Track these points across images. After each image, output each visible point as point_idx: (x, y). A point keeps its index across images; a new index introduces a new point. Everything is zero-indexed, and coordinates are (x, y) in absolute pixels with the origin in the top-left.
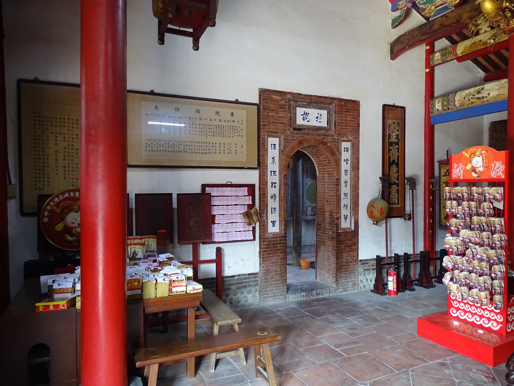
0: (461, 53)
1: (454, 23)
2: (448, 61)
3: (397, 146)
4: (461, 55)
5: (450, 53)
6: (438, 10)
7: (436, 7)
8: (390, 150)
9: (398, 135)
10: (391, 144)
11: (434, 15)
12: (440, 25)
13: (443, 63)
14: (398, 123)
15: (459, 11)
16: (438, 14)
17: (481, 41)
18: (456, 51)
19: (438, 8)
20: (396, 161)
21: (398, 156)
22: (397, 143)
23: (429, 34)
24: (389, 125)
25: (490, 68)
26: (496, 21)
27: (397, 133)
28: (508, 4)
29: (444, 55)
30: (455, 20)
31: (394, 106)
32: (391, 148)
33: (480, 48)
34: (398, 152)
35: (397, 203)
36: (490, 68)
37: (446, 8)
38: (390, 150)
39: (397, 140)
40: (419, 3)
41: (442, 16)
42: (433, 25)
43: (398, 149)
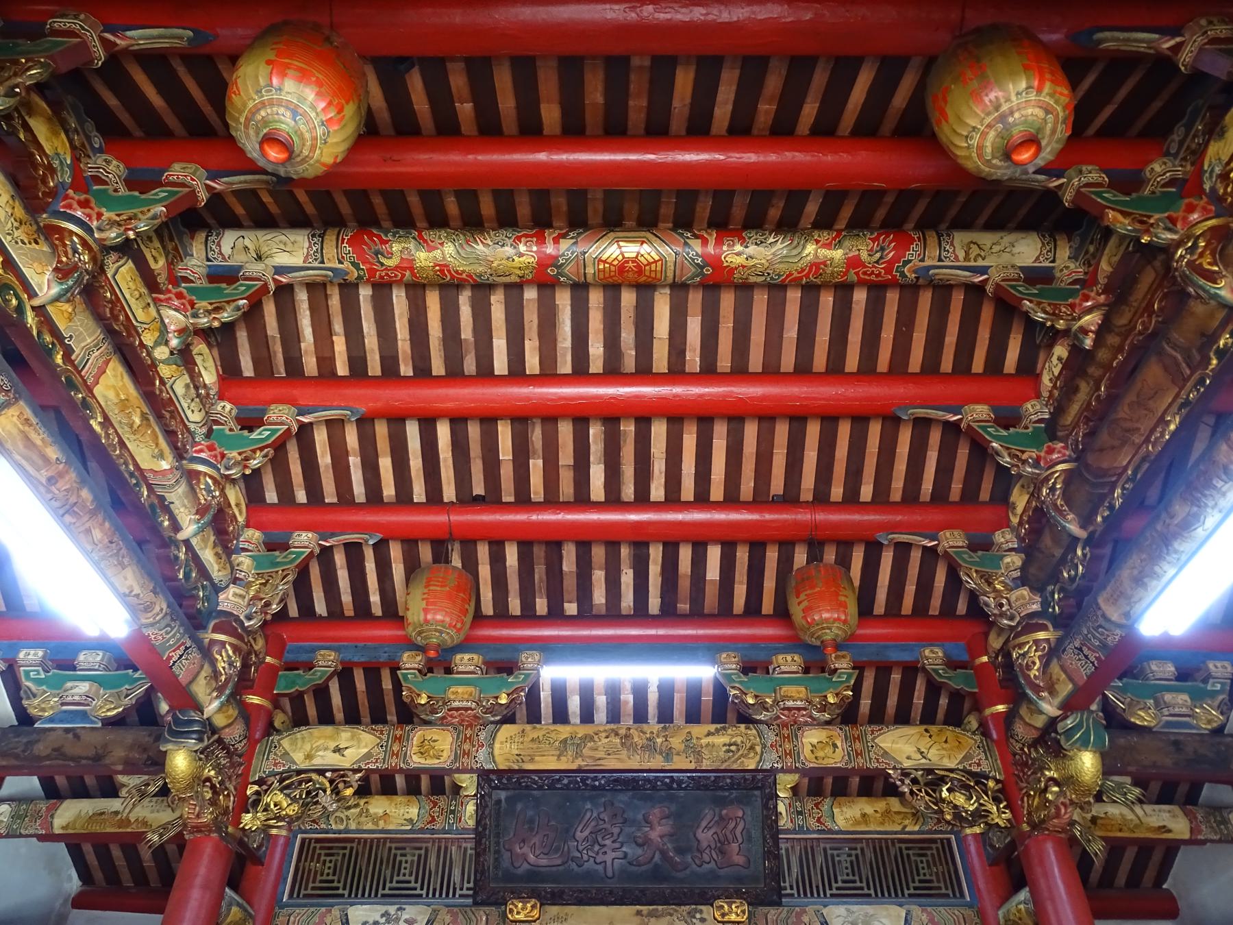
0: (63, 828)
1: (87, 758)
2: (21, 836)
4: (61, 832)
5: (37, 815)
6: (65, 712)
7: (63, 704)
11: (51, 720)
12: (54, 750)
13: (8, 836)
15: (111, 735)
16: (61, 721)
17: (117, 813)
18: (52, 816)
19: (65, 708)
23: (17, 757)
25: (98, 875)
26: (180, 799)
28: (212, 773)
29: (19, 817)
30: (91, 753)
33: (109, 830)
36: (98, 875)
37: (84, 716)
40: (27, 673)
41: (67, 730)
42: (38, 741)
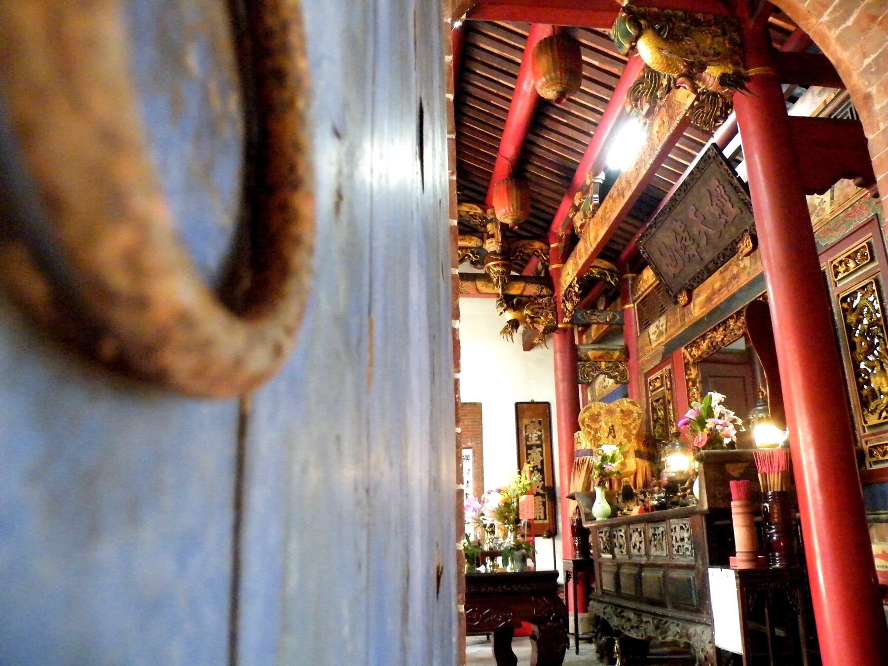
3: (540, 449)
8: (528, 455)
9: (540, 437)
10: (529, 447)
14: (540, 423)
20: (539, 467)
21: (542, 462)
22: (538, 446)
24: (526, 426)
27: (539, 433)
31: (533, 403)
32: (529, 452)
34: (542, 455)
35: (542, 517)
38: (528, 455)
39: (538, 442)
43: (542, 453)
